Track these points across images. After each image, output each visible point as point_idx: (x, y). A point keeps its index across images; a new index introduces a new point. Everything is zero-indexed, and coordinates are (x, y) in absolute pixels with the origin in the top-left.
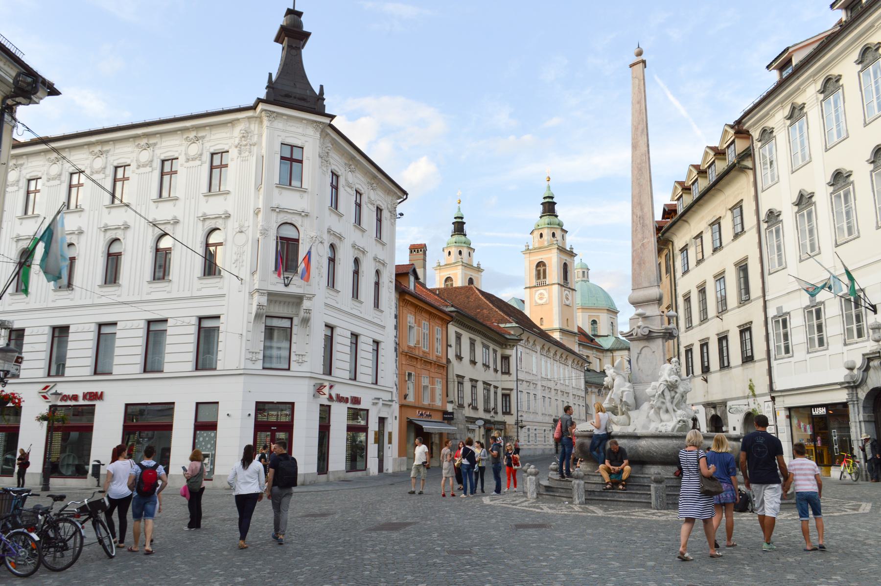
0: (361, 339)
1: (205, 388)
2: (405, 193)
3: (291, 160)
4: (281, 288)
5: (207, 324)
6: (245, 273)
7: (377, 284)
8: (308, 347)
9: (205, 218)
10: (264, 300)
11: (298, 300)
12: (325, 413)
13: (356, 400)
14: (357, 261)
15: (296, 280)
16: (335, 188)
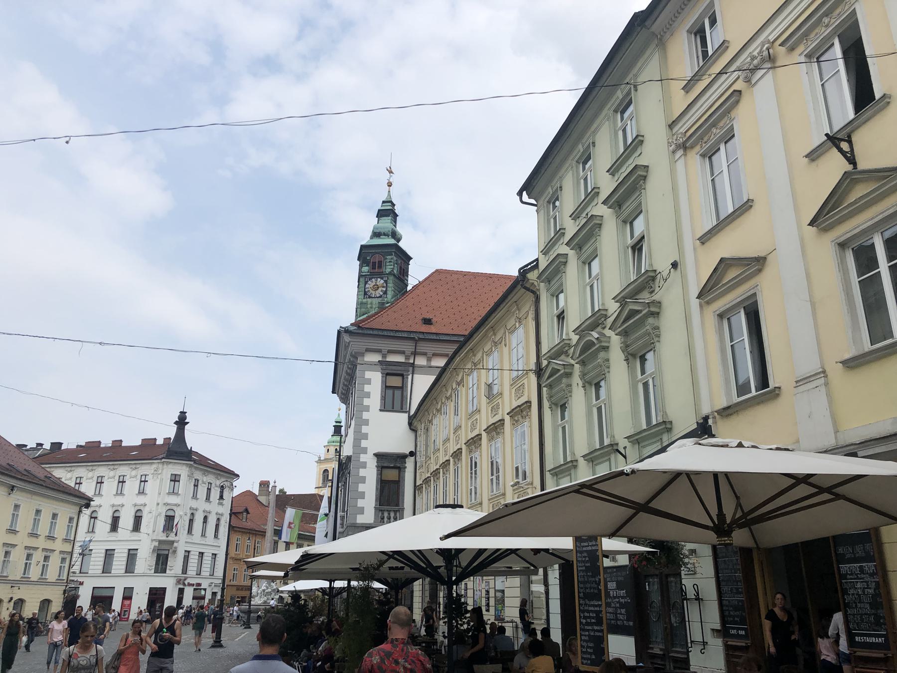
0: (205, 554)
1: (129, 582)
2: (238, 476)
3: (175, 479)
4: (164, 538)
5: (131, 552)
6: (150, 532)
7: (217, 526)
8: (175, 565)
9: (135, 505)
10: (157, 544)
11: (173, 542)
12: (181, 591)
13: (199, 585)
14: (205, 518)
15: (173, 535)
16: (196, 486)
